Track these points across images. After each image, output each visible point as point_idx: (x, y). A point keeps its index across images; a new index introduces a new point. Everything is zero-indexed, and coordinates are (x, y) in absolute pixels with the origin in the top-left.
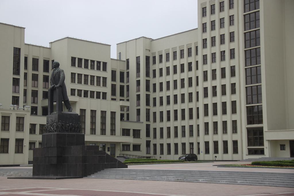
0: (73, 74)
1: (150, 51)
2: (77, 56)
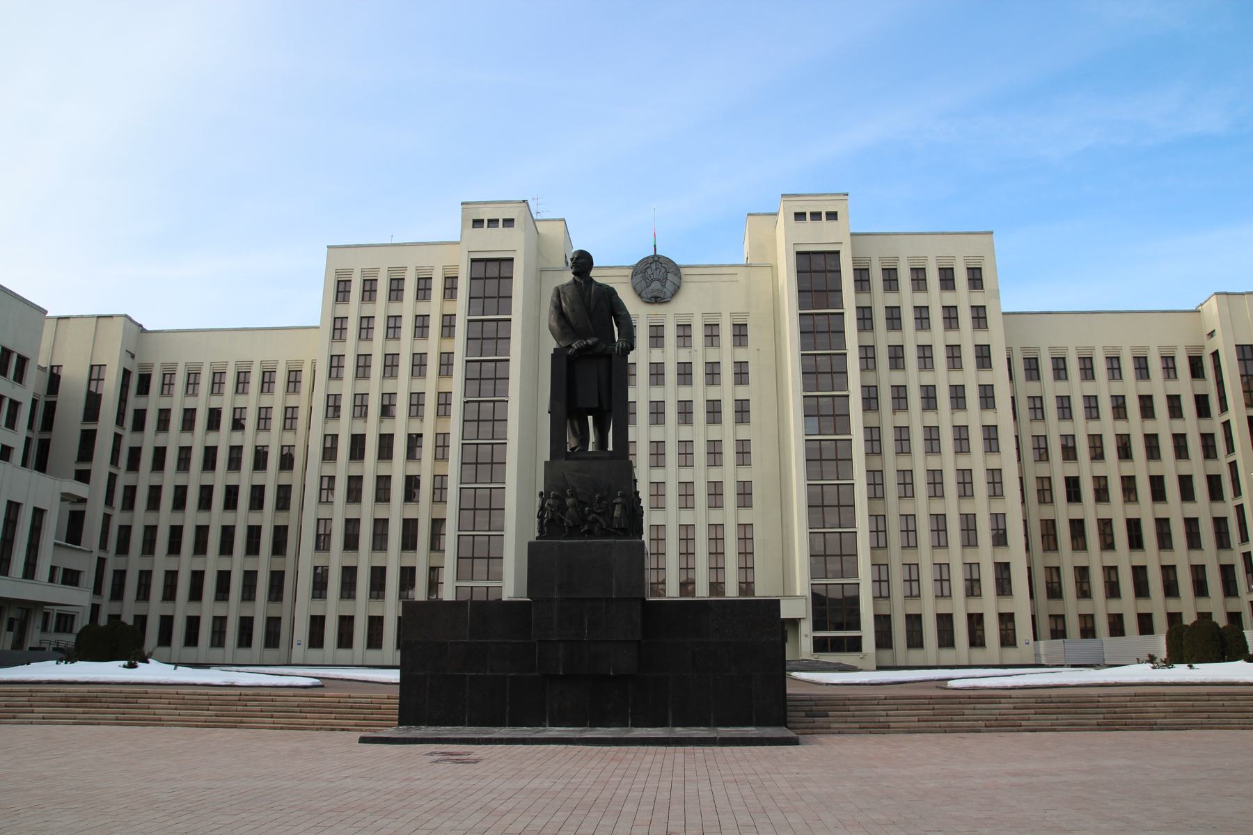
1: (136, 357)
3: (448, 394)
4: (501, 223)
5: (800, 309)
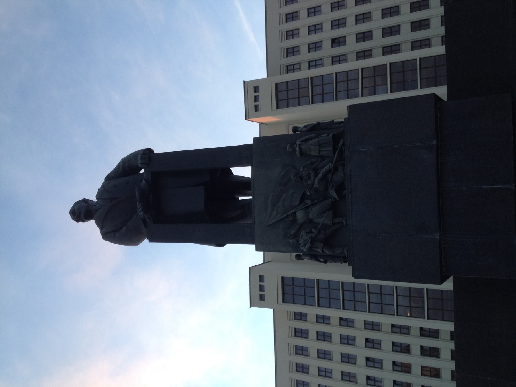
3: (365, 323)
4: (262, 283)
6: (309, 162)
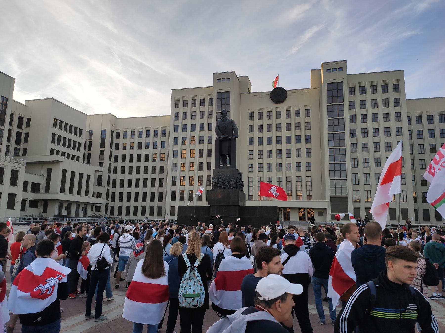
0: (54, 135)
2: (60, 118)
5: (327, 104)
6: (230, 181)
